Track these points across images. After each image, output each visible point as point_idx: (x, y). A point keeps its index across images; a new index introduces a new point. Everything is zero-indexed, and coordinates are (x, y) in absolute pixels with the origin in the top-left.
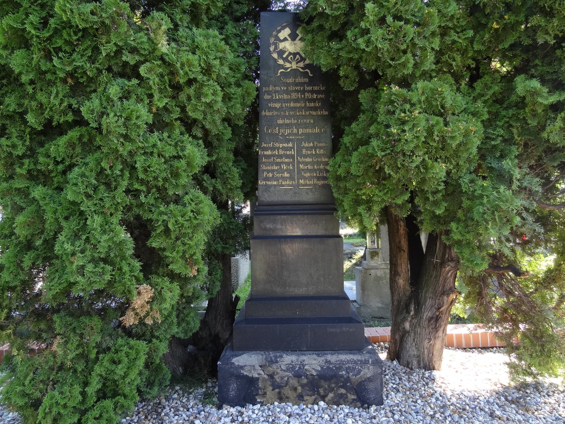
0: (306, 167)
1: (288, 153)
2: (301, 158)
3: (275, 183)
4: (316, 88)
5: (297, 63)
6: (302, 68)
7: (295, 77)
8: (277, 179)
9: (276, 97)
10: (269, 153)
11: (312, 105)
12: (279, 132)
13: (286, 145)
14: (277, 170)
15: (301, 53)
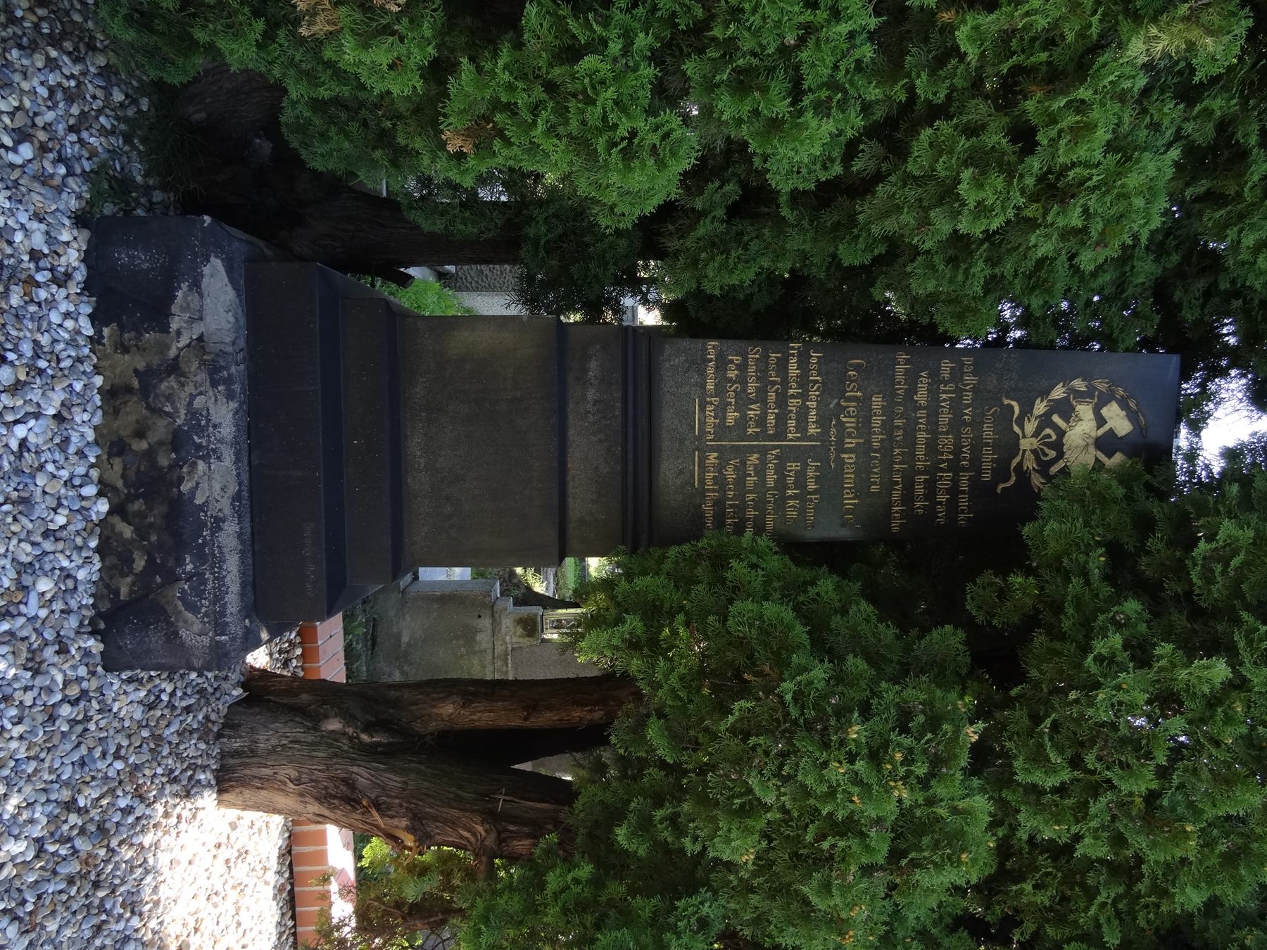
0: (751, 470)
1: (792, 423)
2: (777, 457)
3: (710, 386)
4: (964, 501)
5: (1034, 452)
6: (1020, 464)
7: (996, 446)
8: (720, 391)
9: (944, 392)
10: (793, 370)
11: (920, 490)
12: (849, 399)
13: (812, 416)
14: (744, 390)
15: (1061, 464)
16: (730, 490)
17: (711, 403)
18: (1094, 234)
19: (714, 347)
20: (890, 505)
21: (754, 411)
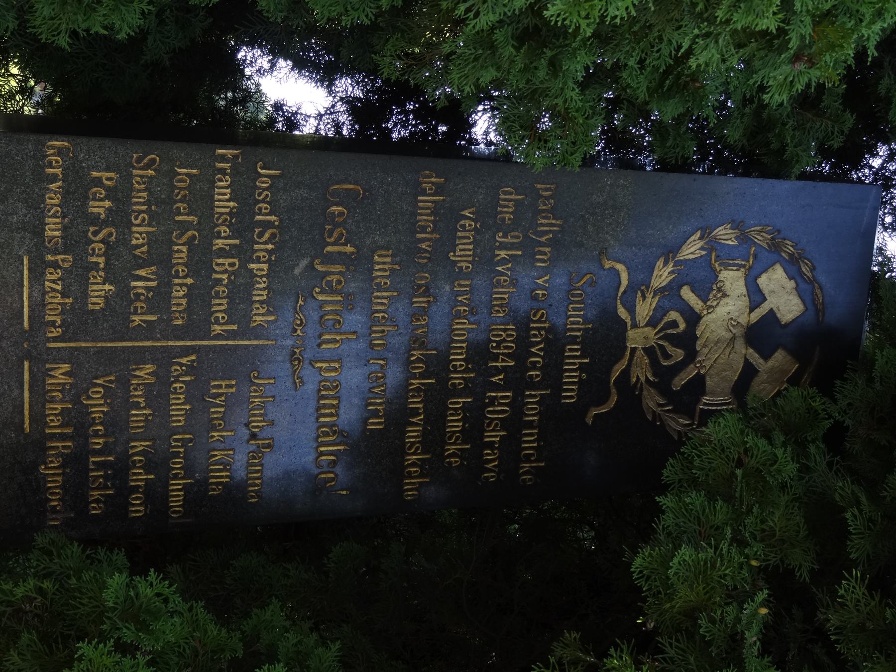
0: (138, 396)
1: (220, 305)
2: (191, 369)
3: (53, 230)
4: (529, 440)
5: (649, 351)
6: (626, 373)
7: (588, 344)
8: (74, 242)
9: (503, 246)
10: (224, 201)
11: (455, 424)
12: (329, 259)
13: (260, 292)
14: (124, 240)
15: (690, 372)
16: (96, 434)
17: (55, 265)
18: (794, 44)
19: (60, 152)
20: (401, 451)
21: (143, 282)
